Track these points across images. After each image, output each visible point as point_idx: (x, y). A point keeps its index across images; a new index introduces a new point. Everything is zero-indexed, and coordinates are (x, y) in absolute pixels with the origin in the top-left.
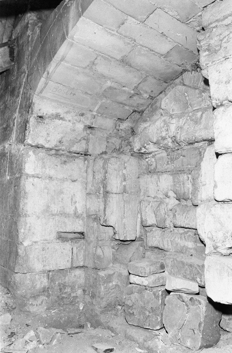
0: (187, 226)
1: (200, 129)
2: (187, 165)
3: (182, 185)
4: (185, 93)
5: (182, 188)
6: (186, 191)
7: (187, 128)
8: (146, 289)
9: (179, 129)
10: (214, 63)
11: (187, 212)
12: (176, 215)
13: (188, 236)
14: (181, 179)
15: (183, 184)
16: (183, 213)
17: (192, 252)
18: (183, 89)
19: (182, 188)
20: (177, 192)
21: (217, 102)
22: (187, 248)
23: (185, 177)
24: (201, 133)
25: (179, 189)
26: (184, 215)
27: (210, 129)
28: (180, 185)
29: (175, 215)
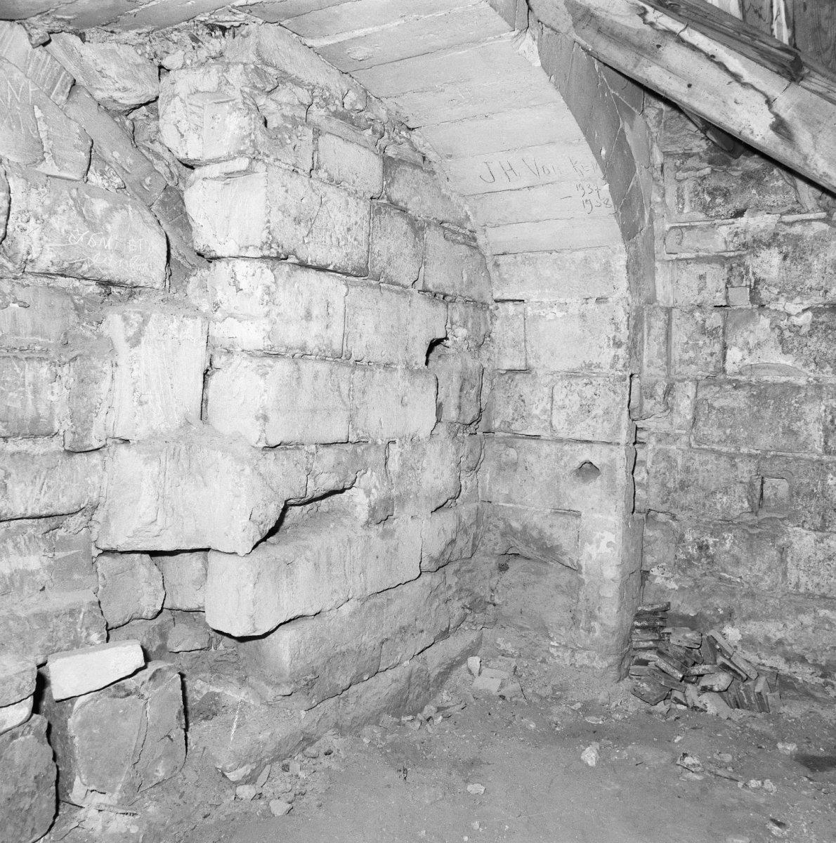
0: (44, 513)
1: (104, 250)
2: (33, 334)
3: (30, 396)
4: (36, 107)
5: (30, 402)
6: (43, 410)
7: (63, 231)
8: (14, 737)
9: (32, 221)
10: (277, 163)
11: (44, 473)
12: (10, 486)
13: (27, 540)
14: (29, 377)
15: (35, 392)
16: (35, 478)
17: (44, 577)
18: (31, 90)
19: (30, 402)
20: (11, 417)
21: (280, 251)
22: (26, 575)
23: (45, 371)
24: (108, 261)
25: (18, 405)
26: (39, 482)
27: (129, 260)
28: (24, 393)
29: (6, 485)
